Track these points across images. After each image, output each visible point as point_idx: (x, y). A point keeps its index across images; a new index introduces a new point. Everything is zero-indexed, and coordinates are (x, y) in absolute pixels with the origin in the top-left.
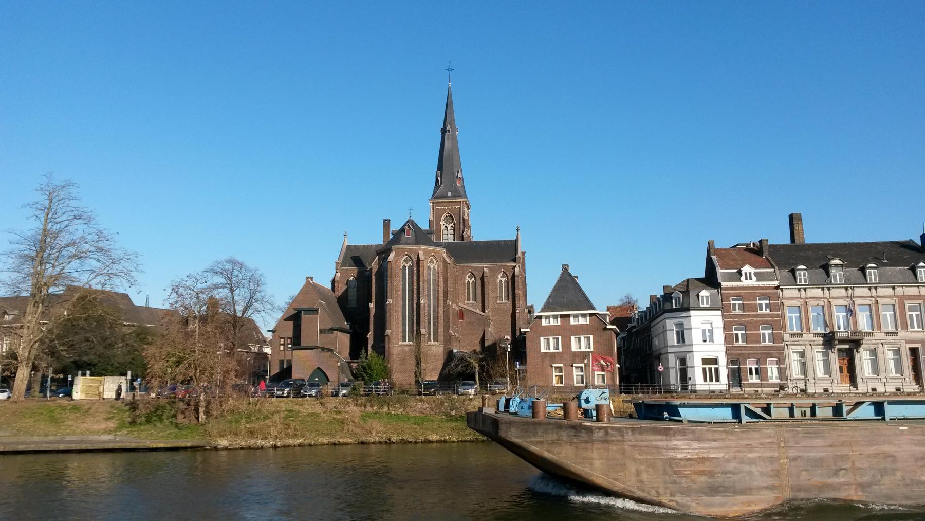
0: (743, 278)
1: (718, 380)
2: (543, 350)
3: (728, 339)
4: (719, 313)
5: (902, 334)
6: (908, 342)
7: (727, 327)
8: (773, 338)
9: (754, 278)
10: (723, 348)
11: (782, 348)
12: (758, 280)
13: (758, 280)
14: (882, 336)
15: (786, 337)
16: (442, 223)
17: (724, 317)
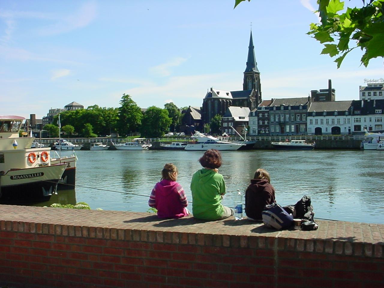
0: (262, 109)
1: (256, 133)
2: (224, 126)
3: (258, 123)
4: (257, 117)
6: (296, 124)
7: (258, 120)
8: (268, 123)
9: (264, 109)
10: (257, 125)
11: (269, 125)
13: (265, 109)
14: (291, 122)
15: (270, 123)
16: (247, 80)
17: (258, 118)
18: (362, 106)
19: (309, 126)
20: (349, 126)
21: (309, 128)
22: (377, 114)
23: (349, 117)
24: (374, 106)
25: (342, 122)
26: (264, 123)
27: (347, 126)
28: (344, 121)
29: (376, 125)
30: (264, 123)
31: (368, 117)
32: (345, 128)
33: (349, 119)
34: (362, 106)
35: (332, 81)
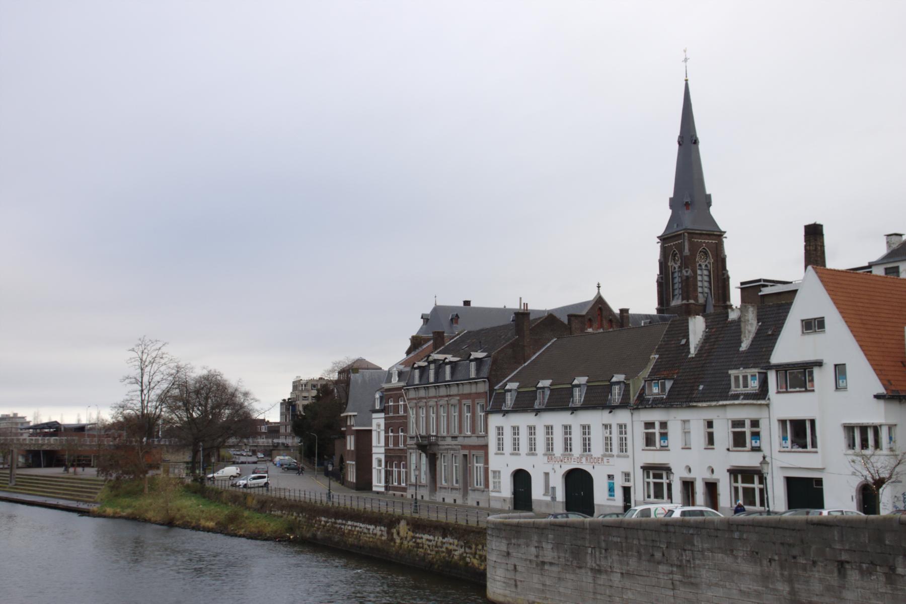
5: (460, 441)
6: (464, 447)
12: (399, 381)
17: (386, 419)
18: (693, 351)
19: (495, 462)
20: (626, 470)
21: (494, 472)
22: (736, 397)
23: (623, 416)
24: (744, 346)
25: (597, 448)
26: (396, 439)
27: (618, 466)
28: (606, 438)
29: (734, 472)
30: (396, 439)
31: (696, 418)
32: (610, 477)
33: (625, 426)
34: (693, 351)
35: (825, 232)
